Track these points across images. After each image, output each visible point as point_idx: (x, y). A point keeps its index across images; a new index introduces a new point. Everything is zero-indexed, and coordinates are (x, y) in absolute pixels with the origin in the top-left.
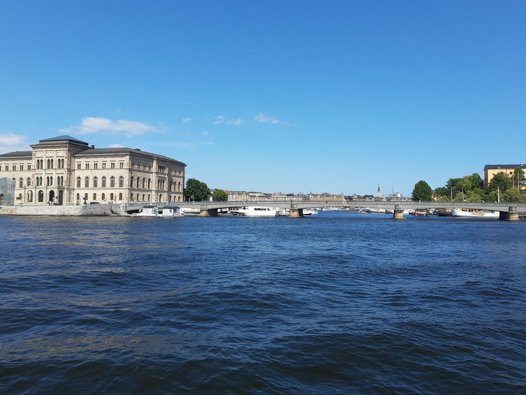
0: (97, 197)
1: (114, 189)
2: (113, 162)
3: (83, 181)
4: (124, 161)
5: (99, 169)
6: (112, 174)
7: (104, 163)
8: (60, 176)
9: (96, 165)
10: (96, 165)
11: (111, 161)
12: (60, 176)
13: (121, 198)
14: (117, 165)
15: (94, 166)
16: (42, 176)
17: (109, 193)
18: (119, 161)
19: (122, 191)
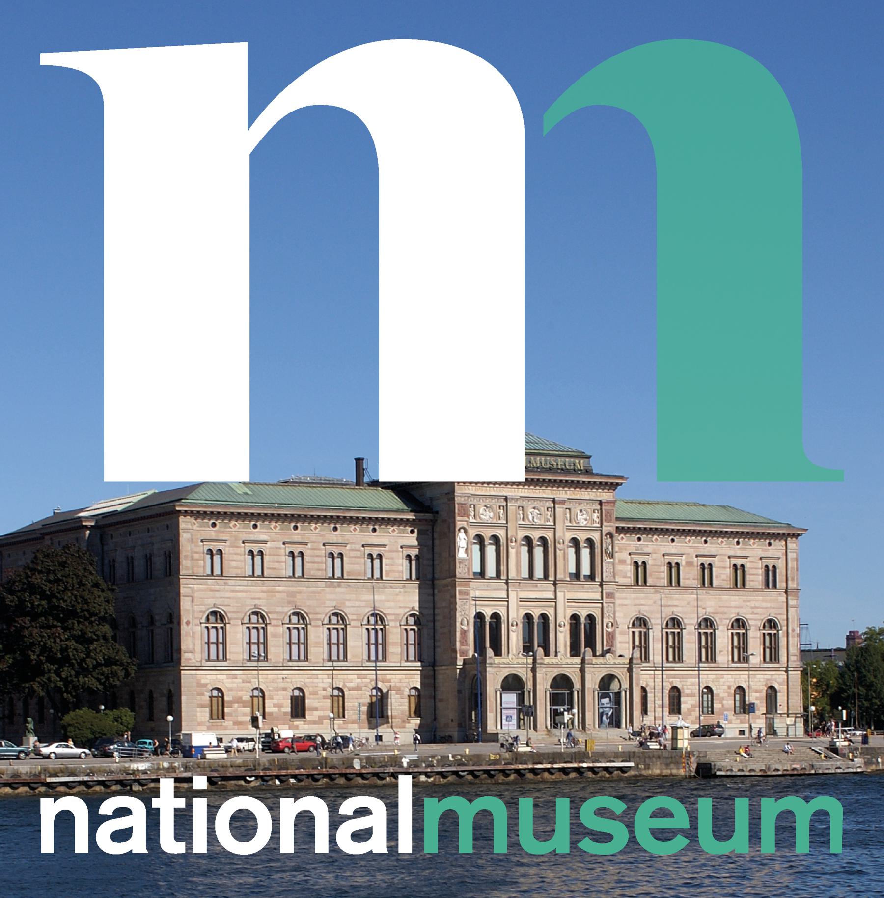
0: (685, 703)
1: (749, 669)
2: (739, 562)
3: (622, 633)
4: (779, 558)
5: (687, 588)
6: (737, 610)
7: (706, 561)
8: (583, 614)
9: (673, 569)
10: (673, 569)
11: (729, 557)
12: (583, 614)
13: (675, 707)
14: (756, 577)
15: (665, 575)
16: (502, 612)
17: (729, 687)
18: (761, 558)
19: (778, 679)
